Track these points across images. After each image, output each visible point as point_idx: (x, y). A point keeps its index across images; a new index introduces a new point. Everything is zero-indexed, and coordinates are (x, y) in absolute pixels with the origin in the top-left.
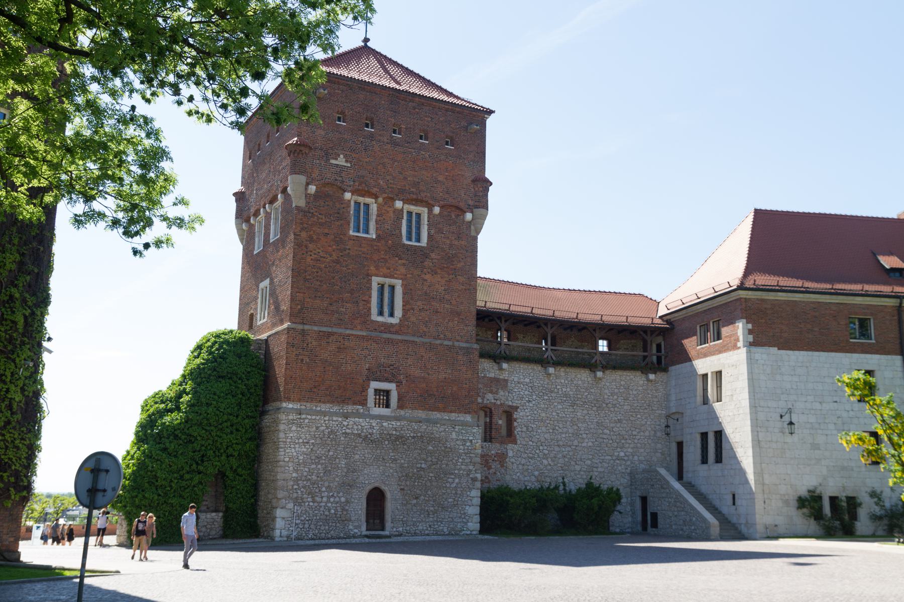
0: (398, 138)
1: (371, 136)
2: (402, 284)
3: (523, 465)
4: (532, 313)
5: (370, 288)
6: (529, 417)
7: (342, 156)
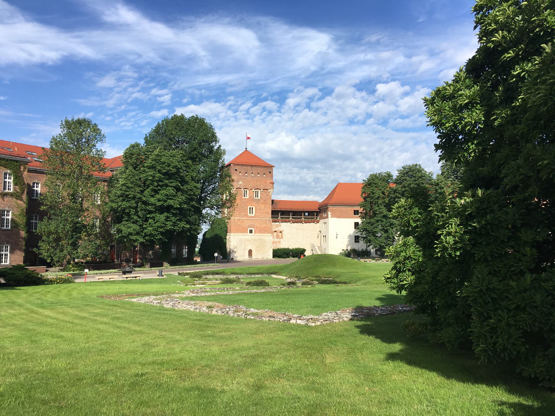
1: (247, 176)
5: (248, 209)
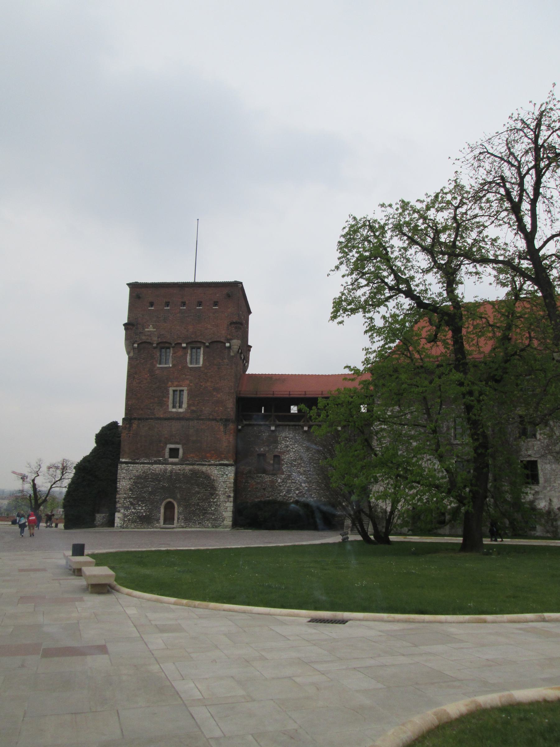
0: (184, 309)
2: (187, 390)
3: (288, 487)
4: (290, 394)
5: (168, 394)
6: (293, 458)
7: (151, 326)
